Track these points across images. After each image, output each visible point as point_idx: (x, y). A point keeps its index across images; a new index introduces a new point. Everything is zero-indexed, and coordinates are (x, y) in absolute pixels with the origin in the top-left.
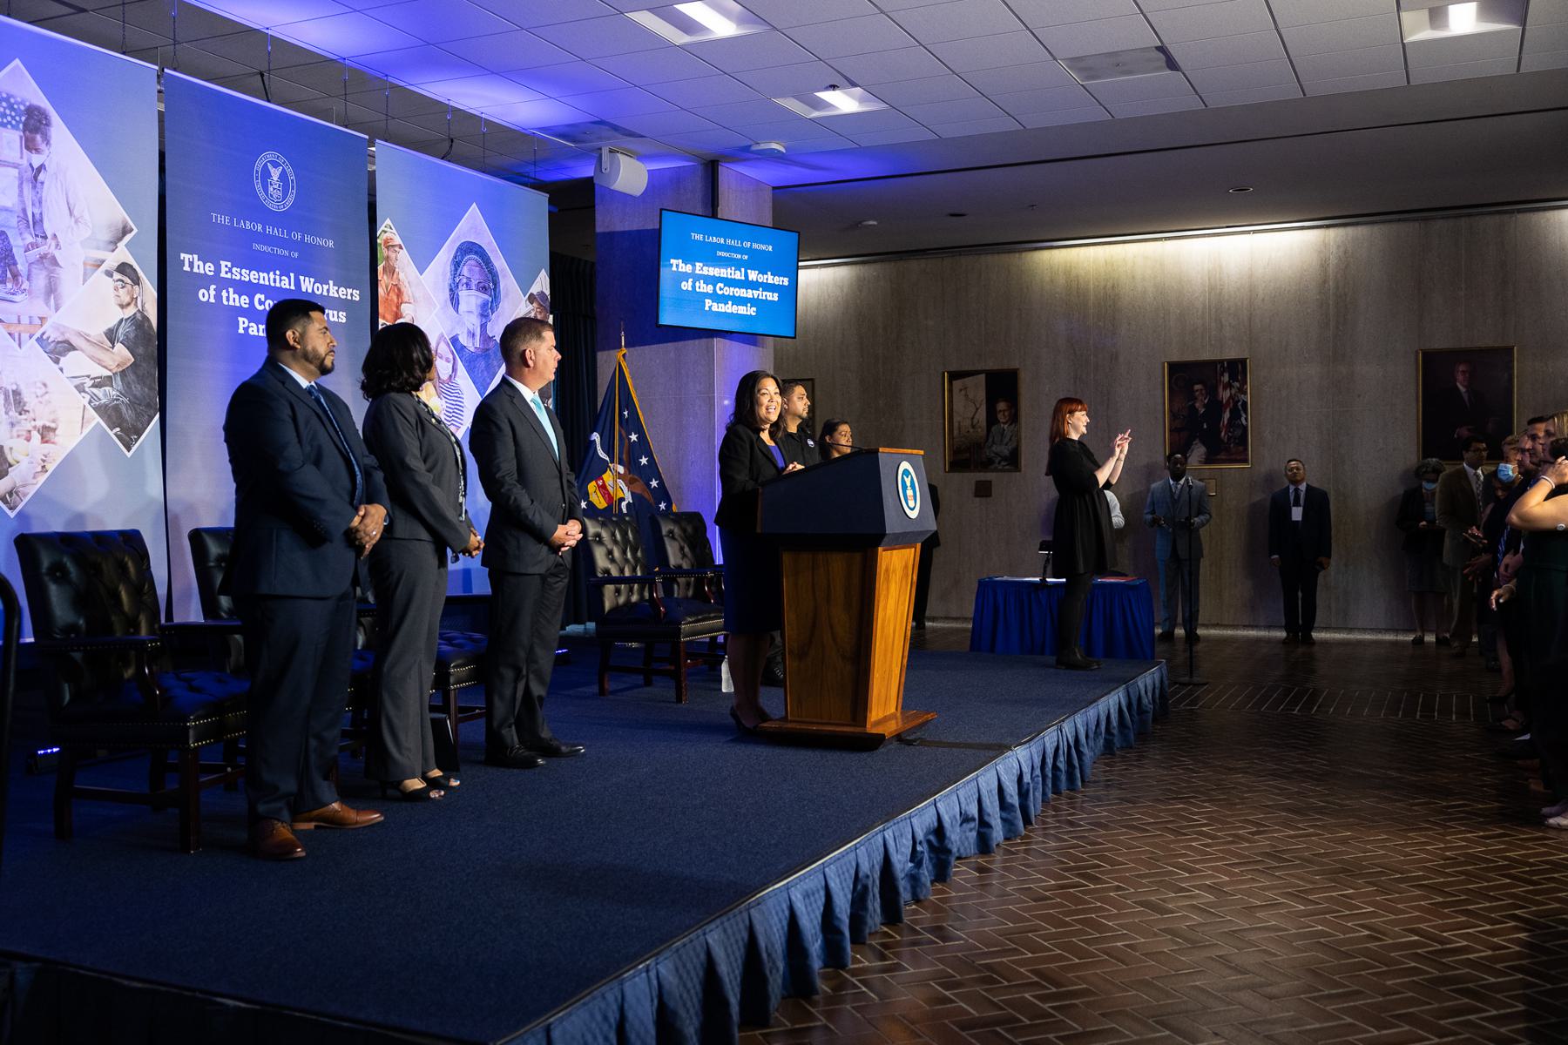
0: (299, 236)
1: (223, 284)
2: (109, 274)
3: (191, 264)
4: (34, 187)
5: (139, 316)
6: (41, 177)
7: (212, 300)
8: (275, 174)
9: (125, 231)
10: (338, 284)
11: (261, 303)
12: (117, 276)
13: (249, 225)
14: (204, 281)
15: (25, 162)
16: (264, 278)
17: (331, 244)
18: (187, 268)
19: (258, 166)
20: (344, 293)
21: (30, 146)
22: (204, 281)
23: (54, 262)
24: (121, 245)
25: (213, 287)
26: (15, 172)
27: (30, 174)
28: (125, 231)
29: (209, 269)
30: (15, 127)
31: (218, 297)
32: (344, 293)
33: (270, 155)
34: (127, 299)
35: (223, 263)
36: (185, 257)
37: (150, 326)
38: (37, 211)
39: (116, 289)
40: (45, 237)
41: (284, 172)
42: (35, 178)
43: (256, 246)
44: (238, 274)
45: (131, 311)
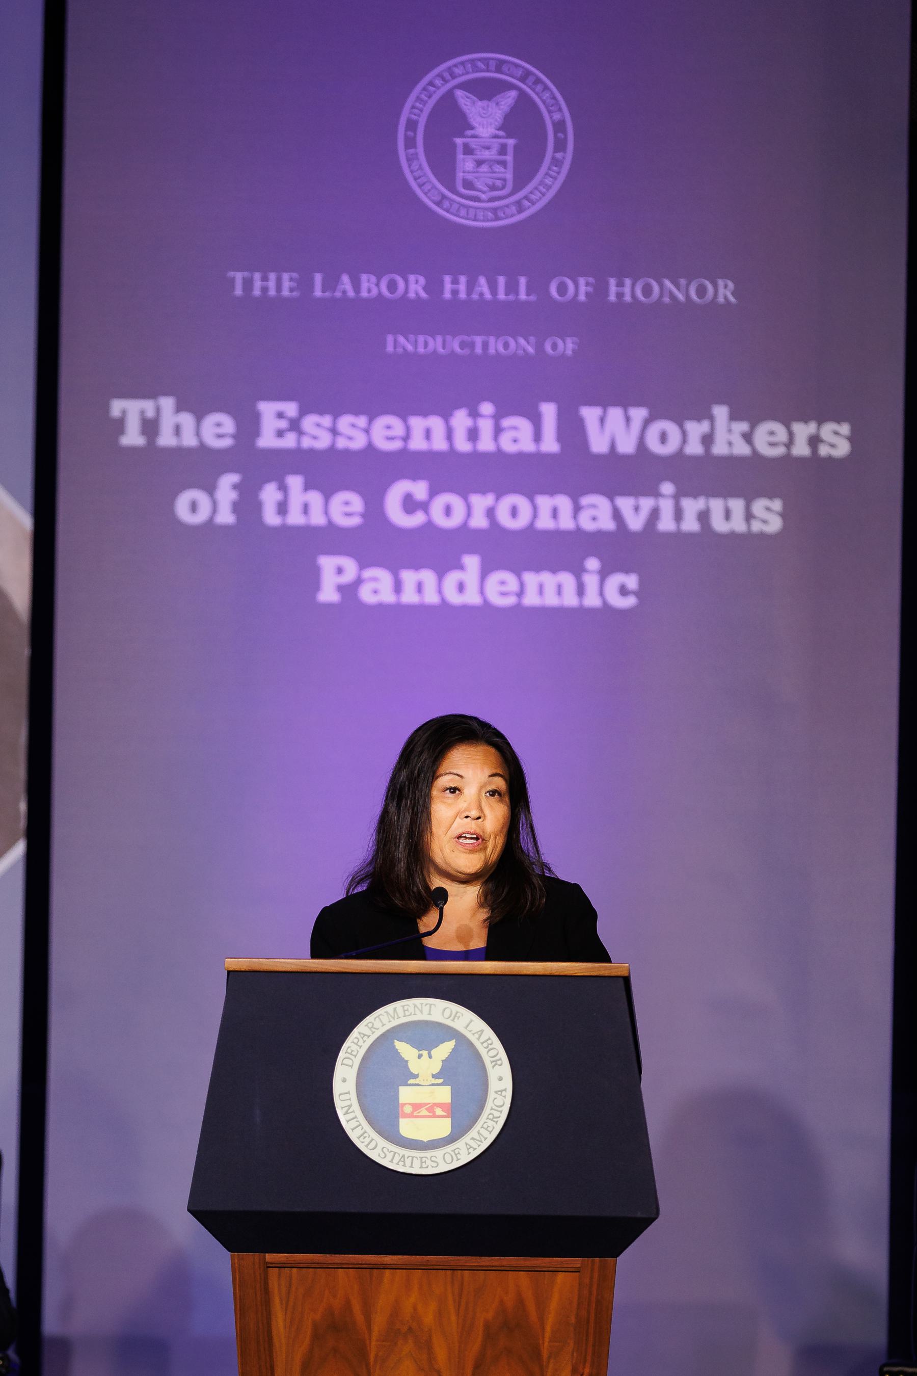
0: (582, 289)
1: (256, 466)
3: (150, 427)
7: (225, 517)
8: (485, 119)
10: (748, 412)
11: (410, 504)
13: (370, 286)
14: (201, 467)
16: (427, 433)
17: (725, 291)
18: (132, 437)
19: (418, 106)
20: (770, 439)
22: (201, 467)
25: (227, 484)
29: (218, 430)
31: (247, 504)
32: (770, 439)
33: (464, 66)
35: (267, 409)
36: (130, 410)
41: (524, 105)
43: (397, 343)
44: (317, 432)
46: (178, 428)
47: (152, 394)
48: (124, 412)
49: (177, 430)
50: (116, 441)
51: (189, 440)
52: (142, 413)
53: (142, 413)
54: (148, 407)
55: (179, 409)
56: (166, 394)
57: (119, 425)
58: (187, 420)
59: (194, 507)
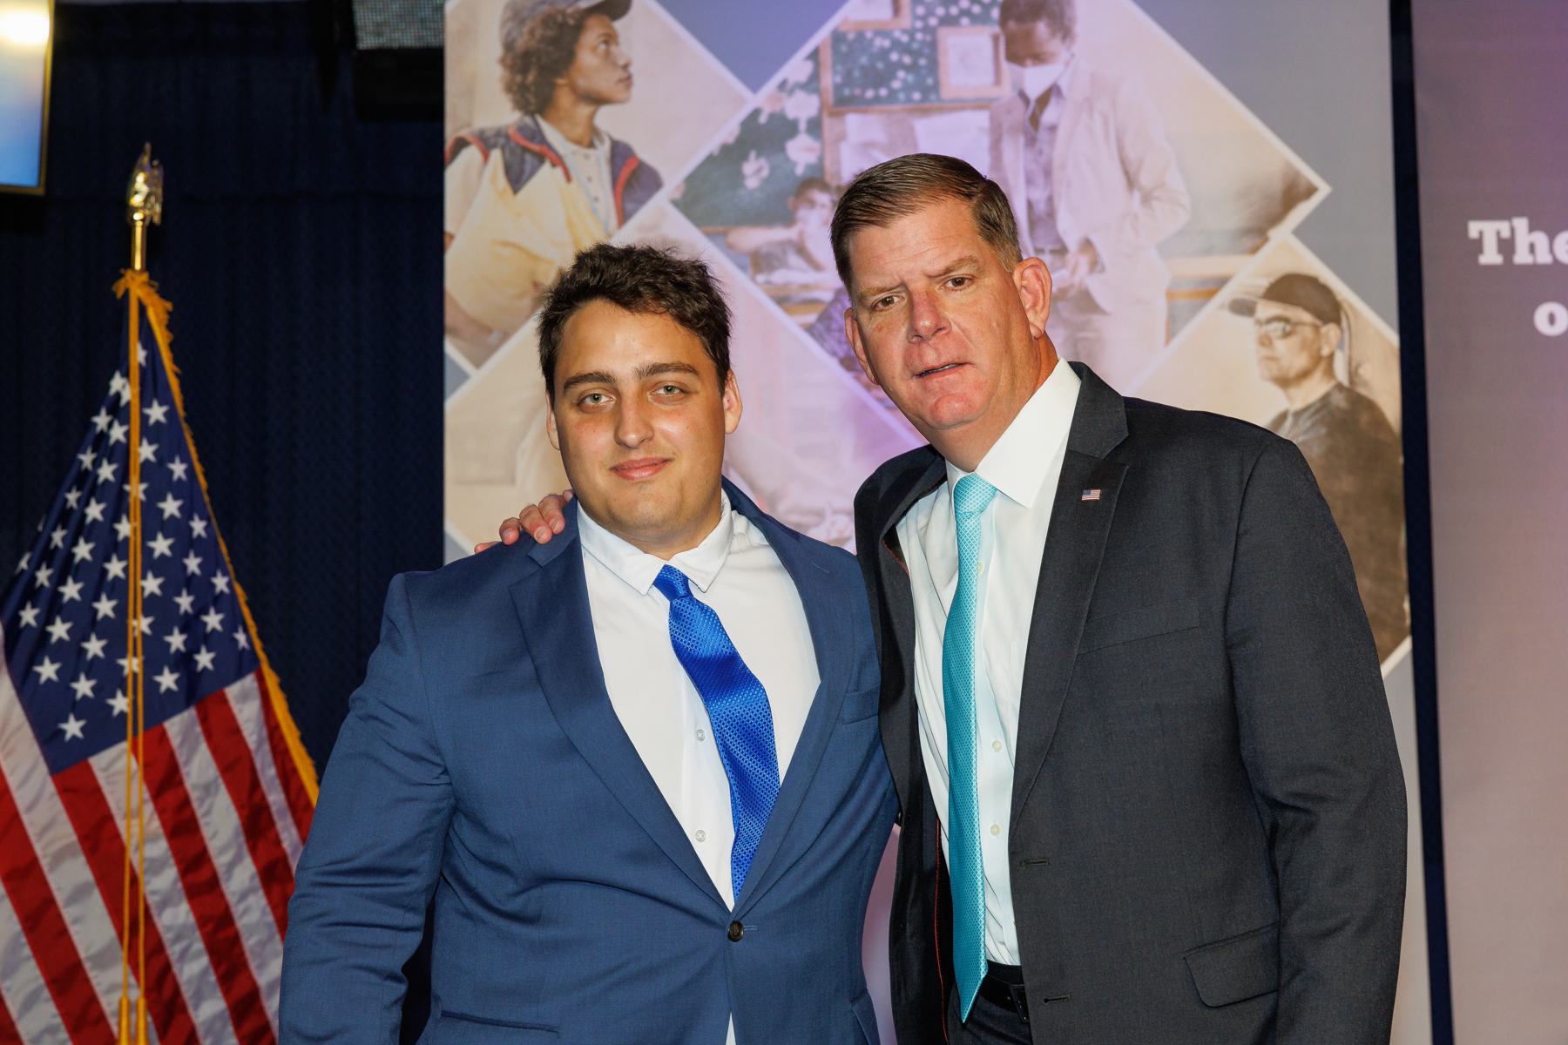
2: (1243, 308)
3: (1507, 246)
4: (1031, 141)
5: (1339, 400)
6: (1049, 116)
9: (1293, 193)
12: (1266, 310)
15: (1006, 92)
18: (1490, 256)
21: (1020, 50)
23: (1086, 302)
24: (1282, 234)
26: (982, 119)
27: (1020, 114)
28: (1293, 193)
30: (976, 20)
34: (1301, 361)
36: (1487, 231)
37: (1379, 419)
38: (1039, 195)
39: (1265, 341)
40: (1062, 251)
42: (1035, 120)
45: (1314, 390)
46: (1532, 246)
47: (1506, 216)
48: (1481, 233)
49: (1532, 248)
50: (1476, 260)
51: (1544, 257)
52: (1498, 233)
53: (1498, 233)
54: (1503, 227)
55: (1532, 229)
56: (1520, 215)
57: (1477, 246)
58: (1540, 238)
59: (1552, 319)
